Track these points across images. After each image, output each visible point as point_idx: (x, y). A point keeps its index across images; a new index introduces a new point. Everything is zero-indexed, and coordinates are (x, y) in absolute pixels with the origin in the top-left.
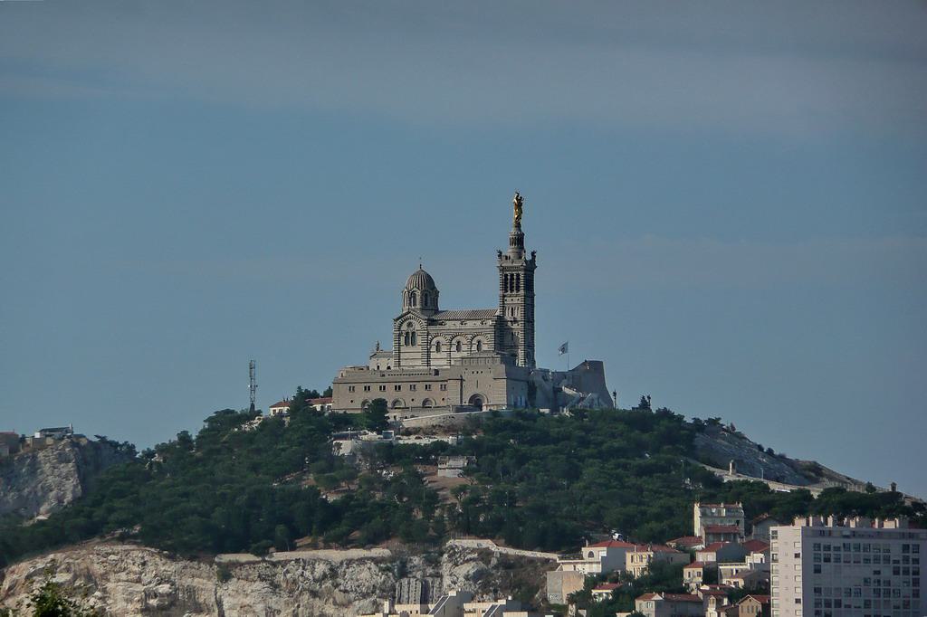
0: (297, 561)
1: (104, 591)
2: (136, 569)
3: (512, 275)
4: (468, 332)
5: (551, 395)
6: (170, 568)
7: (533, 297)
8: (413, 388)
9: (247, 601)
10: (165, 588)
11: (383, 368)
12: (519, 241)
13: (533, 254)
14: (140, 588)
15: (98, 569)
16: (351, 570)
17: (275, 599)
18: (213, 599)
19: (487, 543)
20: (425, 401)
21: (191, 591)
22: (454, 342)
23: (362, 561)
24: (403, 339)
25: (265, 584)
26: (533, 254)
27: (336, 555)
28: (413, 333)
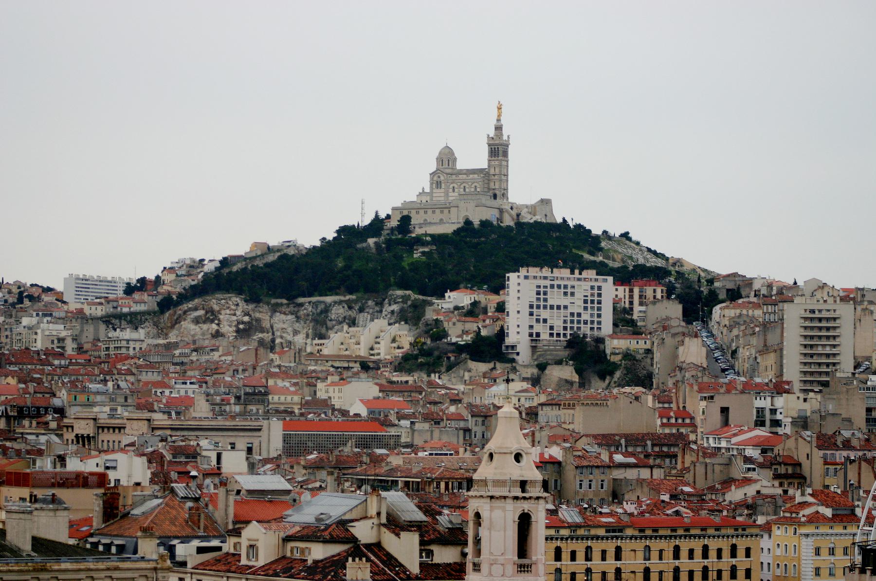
0: (310, 303)
1: (219, 320)
5: (515, 217)
7: (507, 161)
8: (434, 212)
9: (285, 326)
10: (246, 319)
11: (424, 201)
12: (499, 128)
13: (508, 136)
14: (235, 318)
15: (216, 308)
17: (298, 324)
18: (269, 325)
20: (441, 220)
21: (258, 320)
23: (341, 302)
24: (434, 185)
25: (294, 316)
27: (329, 299)
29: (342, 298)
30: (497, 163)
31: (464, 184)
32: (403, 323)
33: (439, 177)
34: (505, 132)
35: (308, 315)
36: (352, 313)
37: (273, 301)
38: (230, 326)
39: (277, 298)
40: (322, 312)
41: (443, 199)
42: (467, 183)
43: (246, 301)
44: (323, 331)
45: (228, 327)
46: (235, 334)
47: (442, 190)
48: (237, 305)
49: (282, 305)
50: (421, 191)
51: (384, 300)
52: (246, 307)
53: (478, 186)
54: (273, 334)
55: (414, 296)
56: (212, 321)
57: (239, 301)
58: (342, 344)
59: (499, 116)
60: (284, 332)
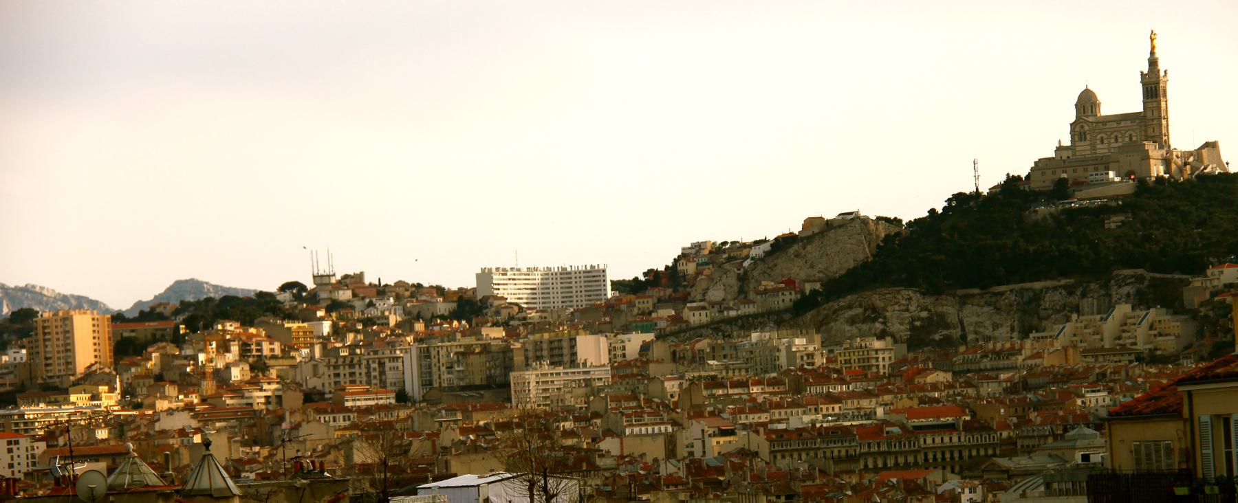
0: (1011, 291)
1: (885, 318)
2: (904, 302)
3: (1151, 87)
4: (1122, 129)
6: (928, 301)
10: (924, 314)
12: (1153, 63)
13: (1165, 72)
14: (907, 314)
15: (880, 304)
16: (1048, 295)
17: (998, 317)
18: (957, 320)
19: (1140, 271)
21: (942, 316)
22: (1113, 136)
23: (1055, 288)
25: (991, 308)
26: (1165, 72)
27: (1038, 285)
28: (1085, 133)
29: (1054, 283)
30: (1155, 105)
31: (1115, 133)
32: (1159, 307)
33: (1082, 127)
34: (1162, 67)
35: (1011, 305)
36: (1074, 300)
37: (960, 292)
38: (901, 324)
39: (964, 288)
40: (1030, 302)
41: (1089, 152)
42: (1118, 131)
43: (923, 294)
44: (1035, 321)
45: (898, 325)
46: (909, 333)
47: (1088, 143)
48: (910, 299)
49: (973, 296)
50: (1058, 146)
51: (1110, 281)
52: (922, 301)
53: (1134, 134)
54: (963, 329)
55: (1148, 275)
56: (874, 320)
57: (911, 294)
58: (1075, 335)
59: (1153, 48)
60: (980, 327)
